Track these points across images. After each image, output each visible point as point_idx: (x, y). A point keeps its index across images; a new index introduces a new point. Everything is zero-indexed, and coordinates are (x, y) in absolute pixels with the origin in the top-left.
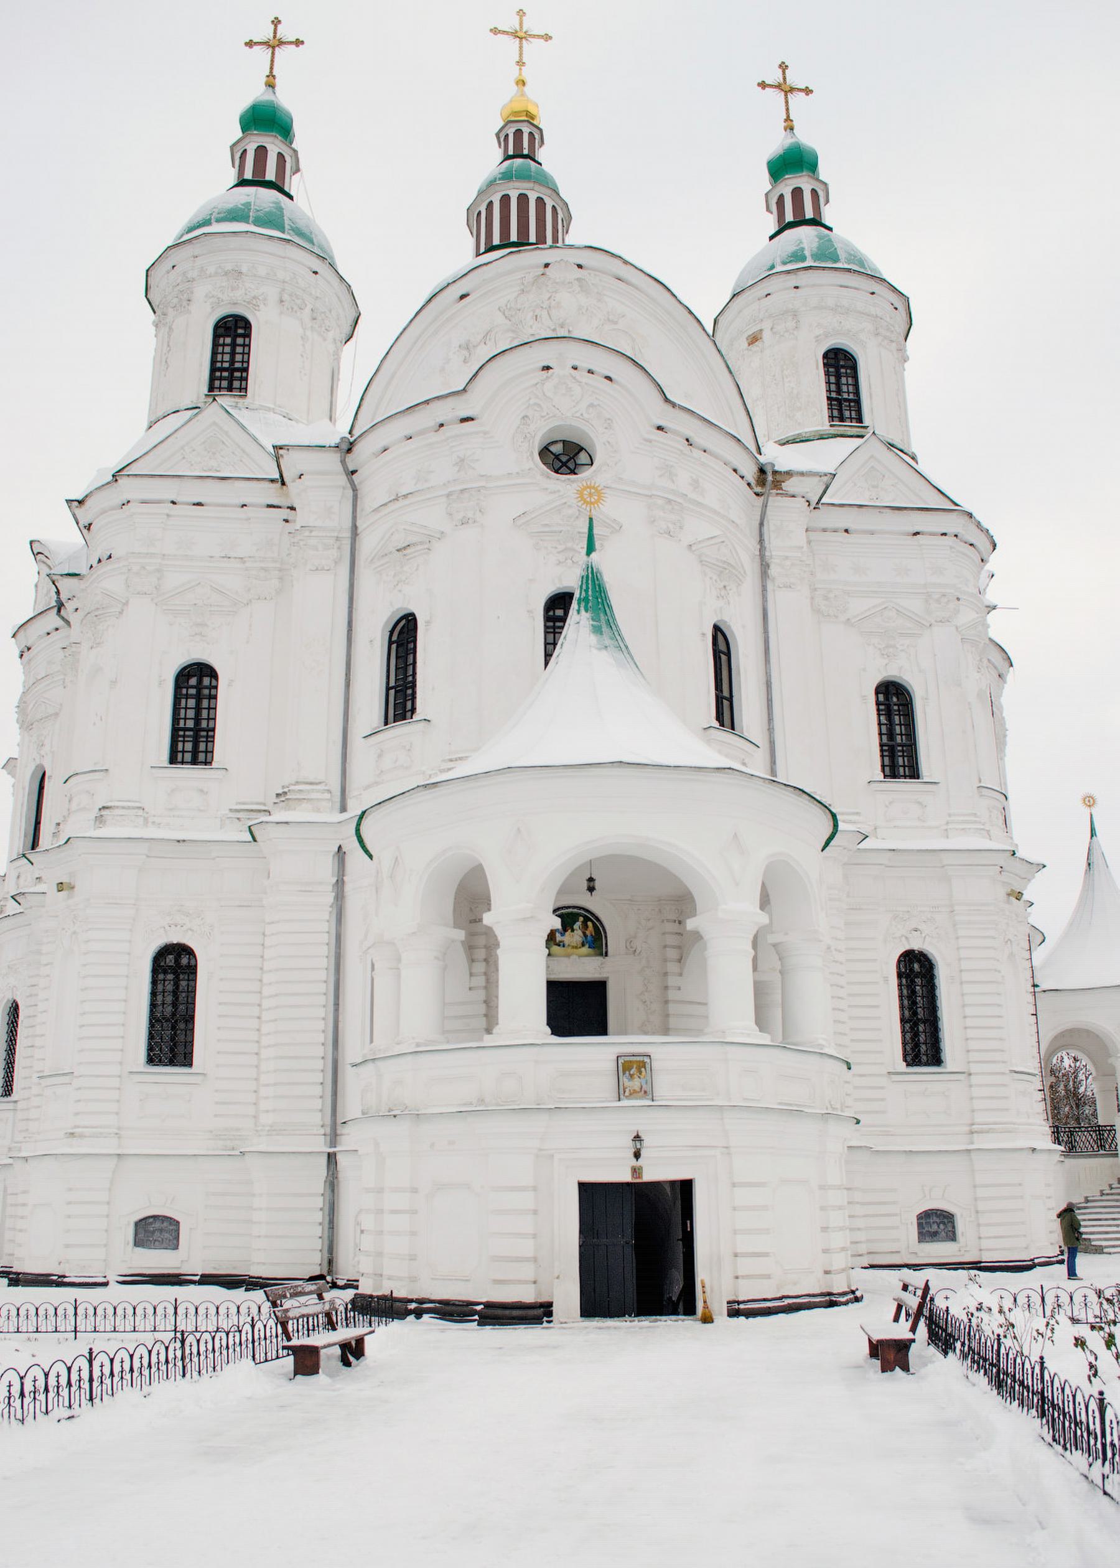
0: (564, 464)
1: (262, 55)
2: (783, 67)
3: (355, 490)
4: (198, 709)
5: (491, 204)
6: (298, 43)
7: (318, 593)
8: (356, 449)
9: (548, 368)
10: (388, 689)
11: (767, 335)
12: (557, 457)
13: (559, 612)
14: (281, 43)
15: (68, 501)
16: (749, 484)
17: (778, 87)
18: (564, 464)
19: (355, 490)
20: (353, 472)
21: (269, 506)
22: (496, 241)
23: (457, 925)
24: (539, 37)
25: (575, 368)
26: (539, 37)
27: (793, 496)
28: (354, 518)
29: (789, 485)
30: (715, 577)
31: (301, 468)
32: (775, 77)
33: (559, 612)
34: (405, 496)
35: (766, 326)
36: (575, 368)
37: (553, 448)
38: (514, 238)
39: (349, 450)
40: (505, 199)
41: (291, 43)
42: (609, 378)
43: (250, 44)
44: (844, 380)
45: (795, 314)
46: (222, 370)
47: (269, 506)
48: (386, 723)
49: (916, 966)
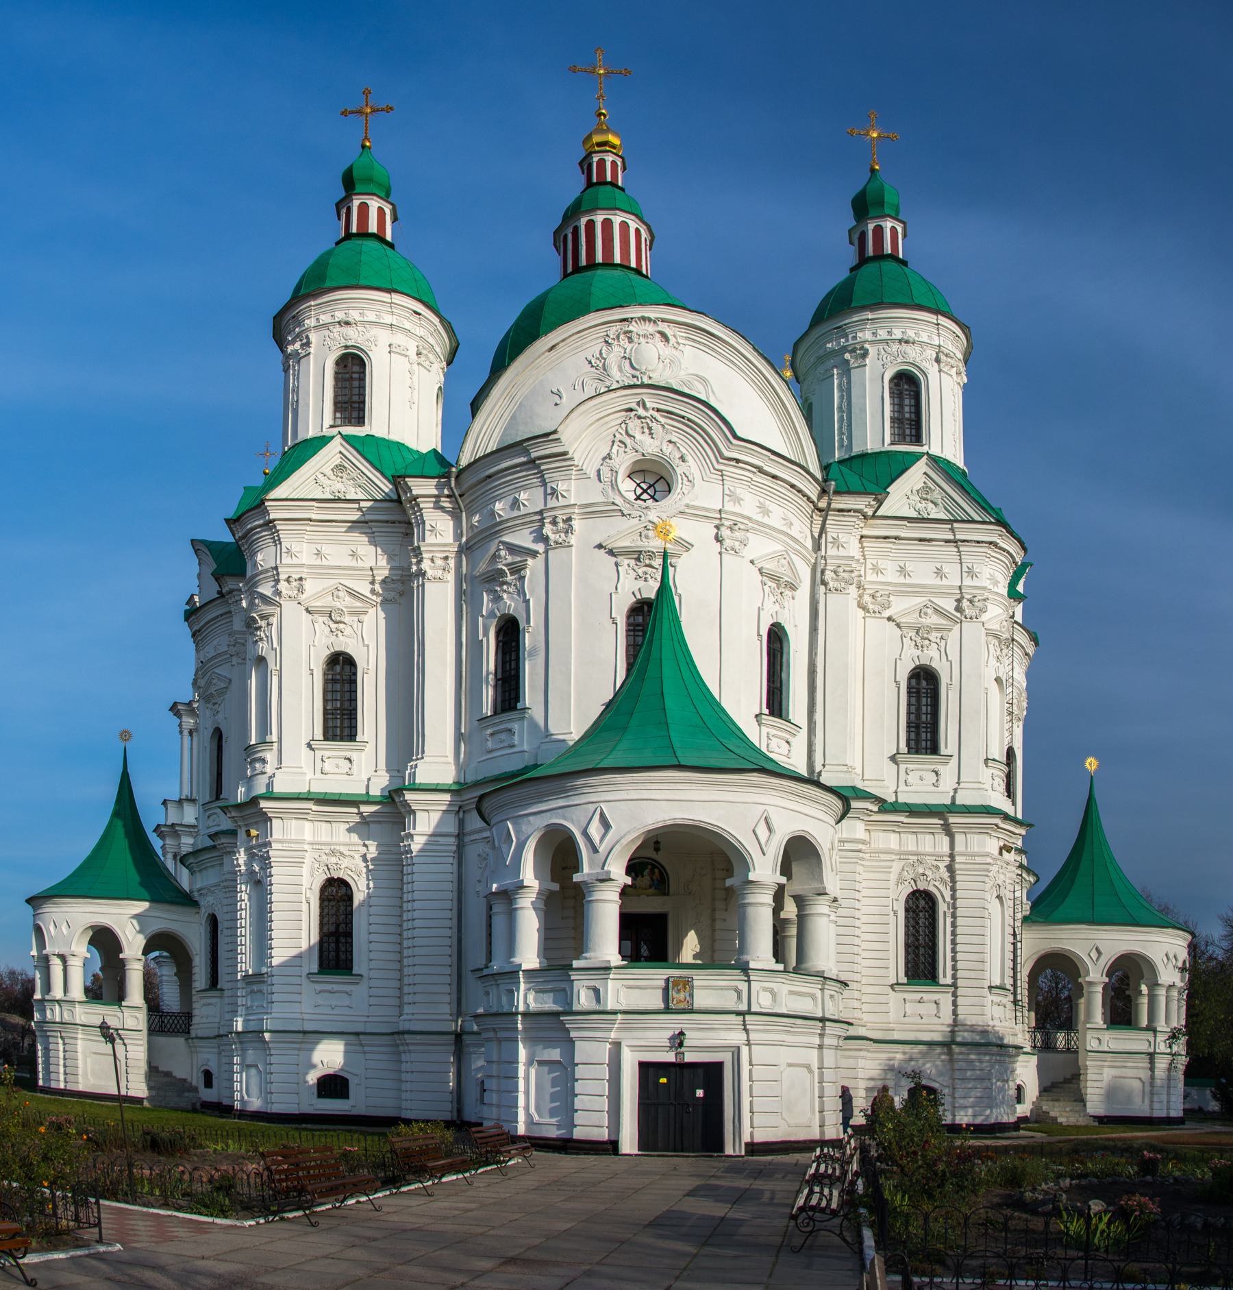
13: (640, 619)
18: (645, 491)
23: (553, 880)
30: (774, 585)
33: (640, 619)
49: (922, 903)
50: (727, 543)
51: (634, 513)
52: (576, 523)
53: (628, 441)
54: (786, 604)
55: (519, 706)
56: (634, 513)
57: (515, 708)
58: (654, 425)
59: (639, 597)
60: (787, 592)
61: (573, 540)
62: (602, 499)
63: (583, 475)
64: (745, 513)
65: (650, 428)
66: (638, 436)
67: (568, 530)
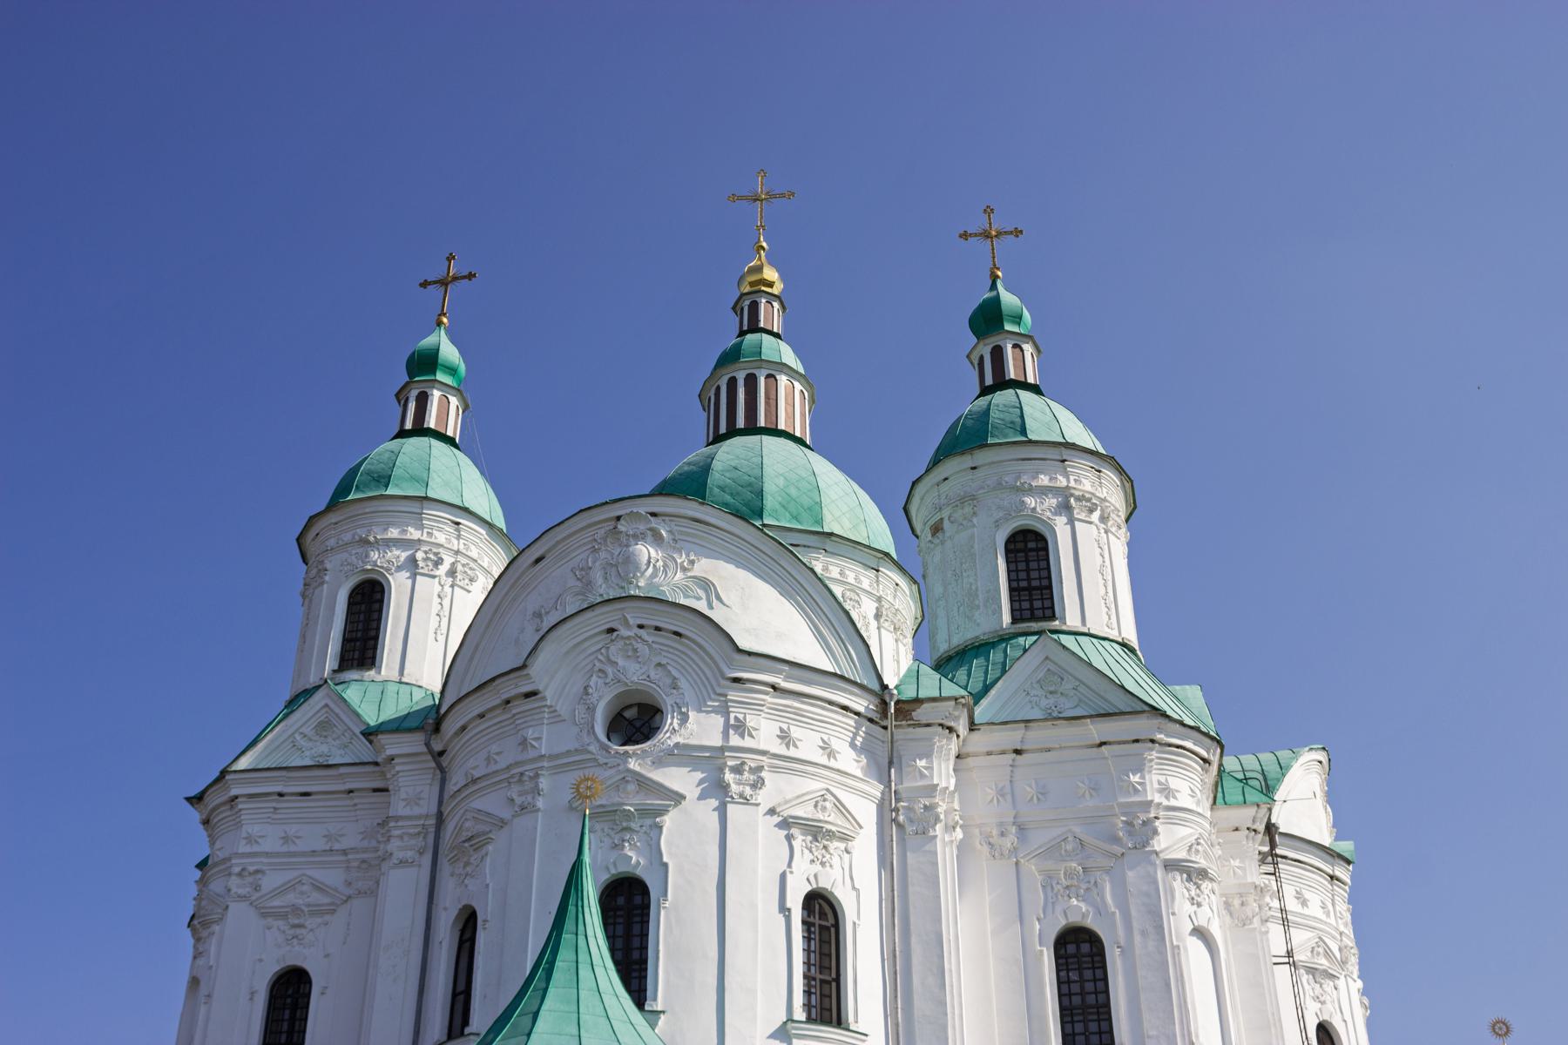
0: (638, 730)
1: (435, 292)
2: (989, 211)
3: (442, 770)
4: (293, 1019)
5: (718, 388)
6: (471, 276)
7: (402, 889)
8: (445, 726)
9: (611, 630)
10: (455, 995)
11: (946, 524)
12: (630, 722)
14: (455, 278)
15: (188, 799)
16: (871, 720)
17: (986, 235)
18: (638, 730)
19: (442, 770)
20: (441, 753)
21: (375, 790)
22: (723, 430)
24: (782, 196)
25: (641, 627)
26: (782, 196)
27: (928, 725)
28: (440, 802)
29: (921, 714)
31: (389, 752)
32: (978, 223)
34: (474, 781)
35: (945, 514)
36: (641, 627)
37: (627, 714)
38: (741, 423)
39: (437, 729)
40: (732, 383)
41: (464, 277)
42: (677, 634)
43: (425, 284)
44: (1033, 565)
45: (973, 498)
46: (355, 640)
47: (375, 790)
48: (450, 1037)
50: (734, 788)
51: (612, 761)
52: (544, 783)
53: (610, 670)
54: (836, 861)
55: (467, 1031)
56: (612, 761)
57: (462, 1034)
58: (639, 646)
59: (613, 871)
60: (835, 845)
61: (540, 803)
62: (572, 745)
63: (556, 718)
64: (762, 747)
65: (635, 650)
66: (621, 662)
67: (537, 791)
